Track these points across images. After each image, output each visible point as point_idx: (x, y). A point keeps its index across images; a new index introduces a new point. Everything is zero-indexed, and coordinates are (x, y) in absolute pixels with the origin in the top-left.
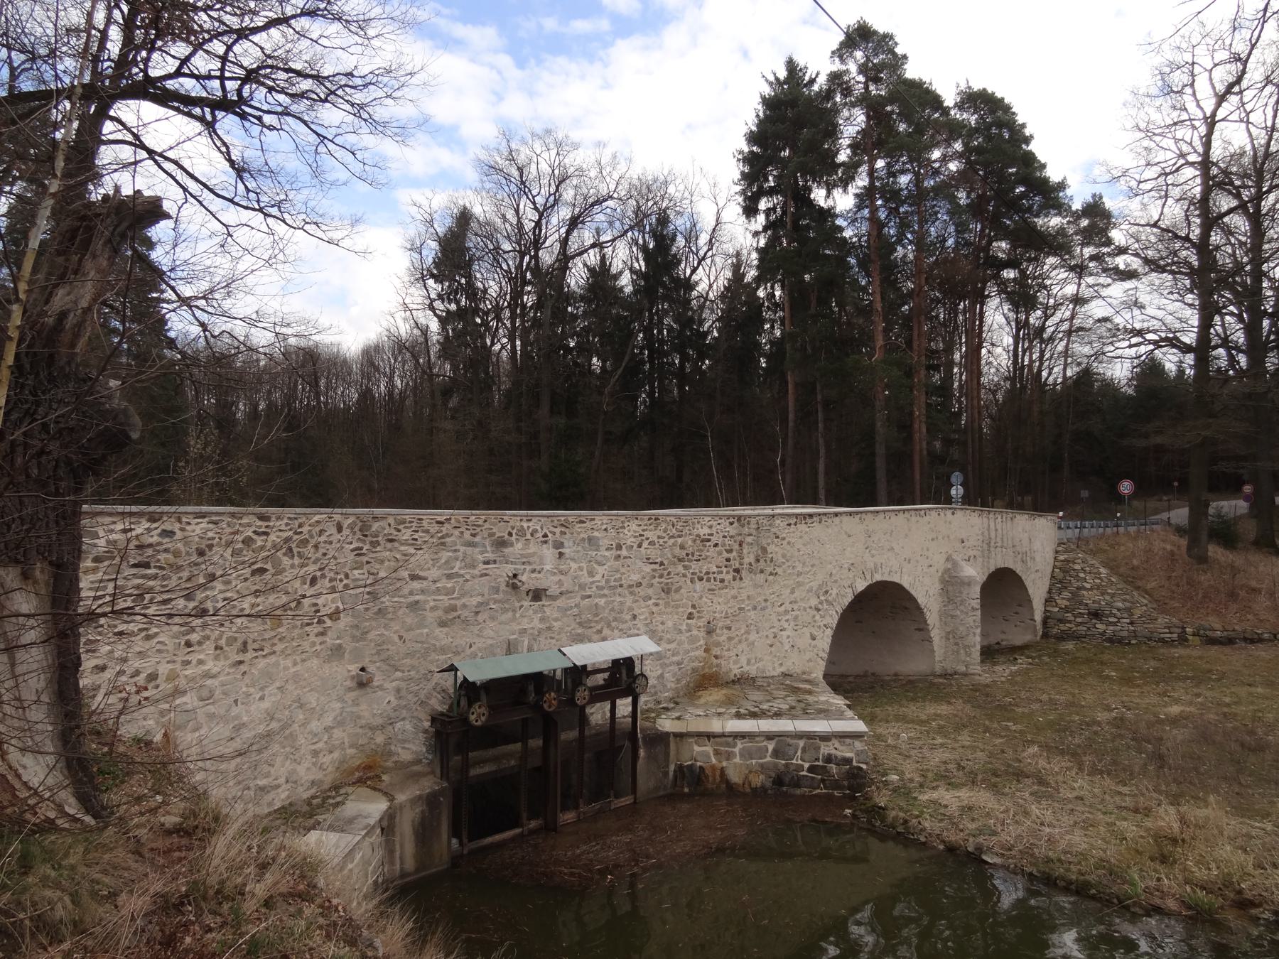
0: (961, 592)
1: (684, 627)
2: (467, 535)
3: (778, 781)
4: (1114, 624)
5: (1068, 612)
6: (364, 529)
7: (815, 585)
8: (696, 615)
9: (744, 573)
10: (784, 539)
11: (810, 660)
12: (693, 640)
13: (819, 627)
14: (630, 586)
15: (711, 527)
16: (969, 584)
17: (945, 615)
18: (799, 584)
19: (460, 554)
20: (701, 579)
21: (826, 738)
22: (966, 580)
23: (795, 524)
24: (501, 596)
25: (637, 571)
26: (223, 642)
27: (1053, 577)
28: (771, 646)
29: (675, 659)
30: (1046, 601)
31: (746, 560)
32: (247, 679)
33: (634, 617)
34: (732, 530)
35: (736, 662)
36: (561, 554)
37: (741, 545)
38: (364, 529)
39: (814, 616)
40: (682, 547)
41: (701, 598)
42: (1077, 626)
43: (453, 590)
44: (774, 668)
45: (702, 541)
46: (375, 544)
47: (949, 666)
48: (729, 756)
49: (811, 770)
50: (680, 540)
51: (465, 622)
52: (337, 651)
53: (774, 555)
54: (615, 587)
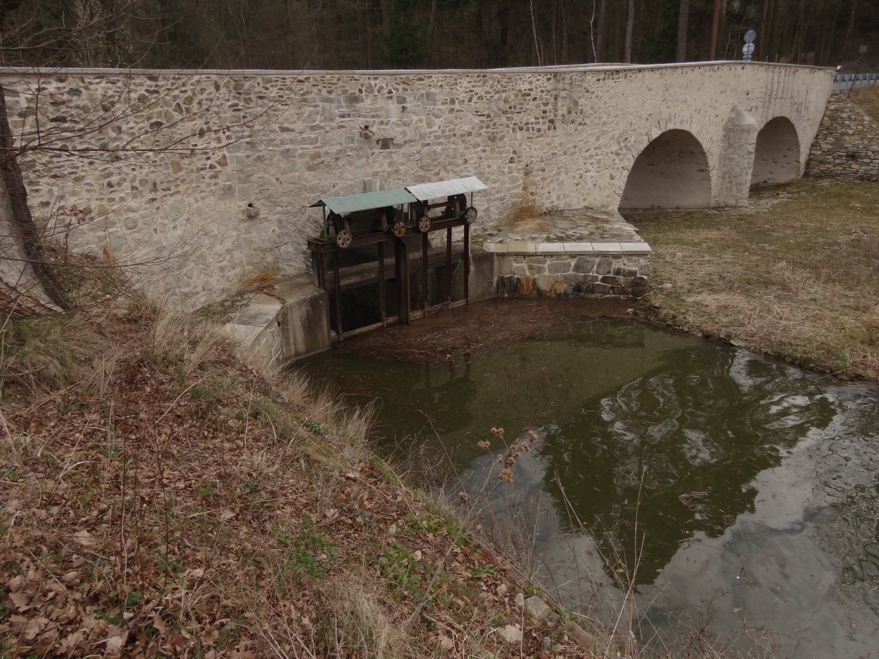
0: (740, 139)
1: (506, 170)
2: (324, 92)
3: (578, 289)
4: (868, 164)
5: (829, 155)
6: (238, 87)
7: (617, 133)
8: (516, 160)
9: (558, 124)
10: (593, 93)
11: (608, 196)
12: (513, 180)
13: (618, 169)
14: (463, 135)
15: (531, 83)
16: (748, 131)
17: (725, 158)
18: (604, 133)
19: (320, 109)
20: (521, 129)
21: (617, 256)
22: (746, 128)
24: (355, 145)
25: (468, 122)
26: (136, 184)
27: (821, 124)
28: (577, 185)
29: (499, 195)
30: (812, 145)
31: (560, 112)
32: (161, 212)
33: (466, 161)
34: (549, 86)
35: (548, 198)
36: (404, 108)
37: (556, 99)
38: (238, 87)
39: (614, 160)
40: (506, 101)
41: (521, 145)
42: (835, 166)
43: (315, 141)
44: (579, 203)
45: (523, 96)
46: (248, 101)
47: (721, 201)
48: (540, 270)
49: (604, 280)
50: (504, 95)
51: (329, 166)
52: (228, 191)
54: (449, 137)
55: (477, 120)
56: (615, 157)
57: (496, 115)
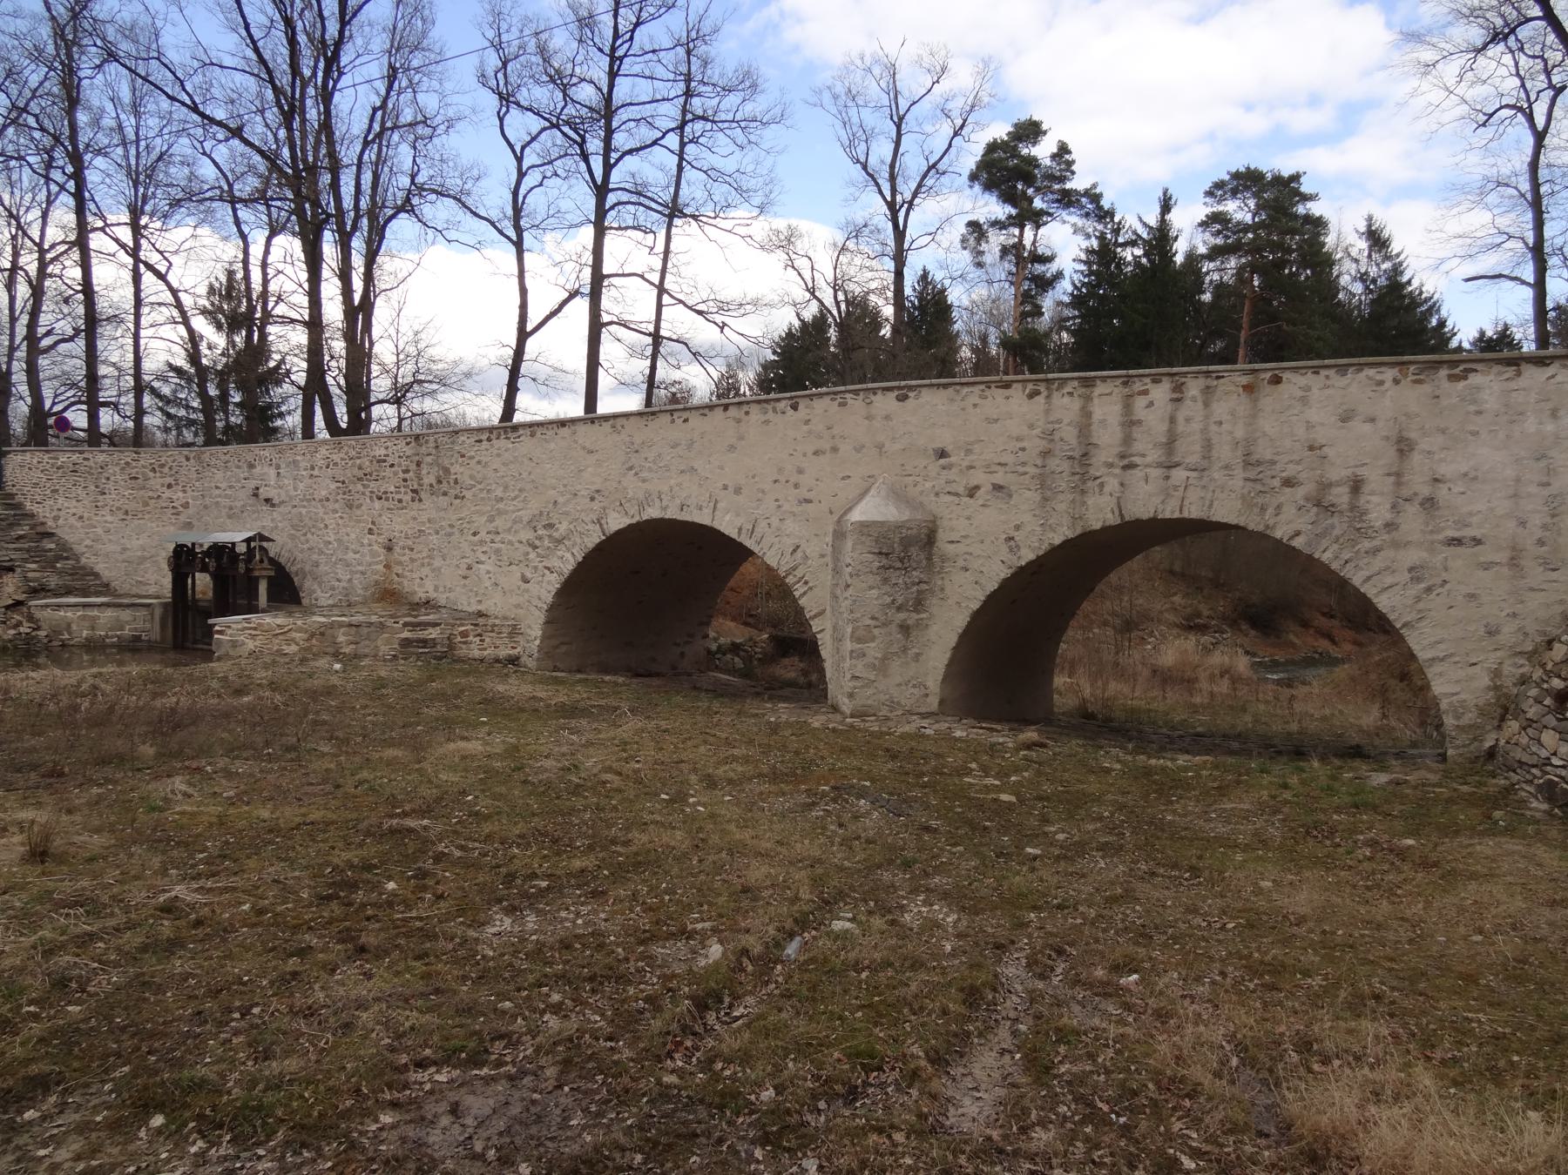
7: (526, 515)
8: (376, 531)
9: (423, 495)
10: (472, 458)
11: (518, 606)
12: (373, 554)
13: (536, 568)
14: (321, 500)
15: (387, 448)
18: (500, 512)
20: (380, 498)
23: (489, 440)
25: (326, 487)
28: (465, 578)
29: (360, 568)
31: (426, 481)
33: (326, 526)
34: (409, 451)
35: (420, 586)
37: (418, 464)
39: (528, 554)
40: (360, 468)
41: (380, 515)
44: (469, 604)
45: (379, 461)
50: (358, 461)
53: (459, 477)
54: (308, 501)
55: (333, 486)
56: (530, 550)
57: (350, 482)
